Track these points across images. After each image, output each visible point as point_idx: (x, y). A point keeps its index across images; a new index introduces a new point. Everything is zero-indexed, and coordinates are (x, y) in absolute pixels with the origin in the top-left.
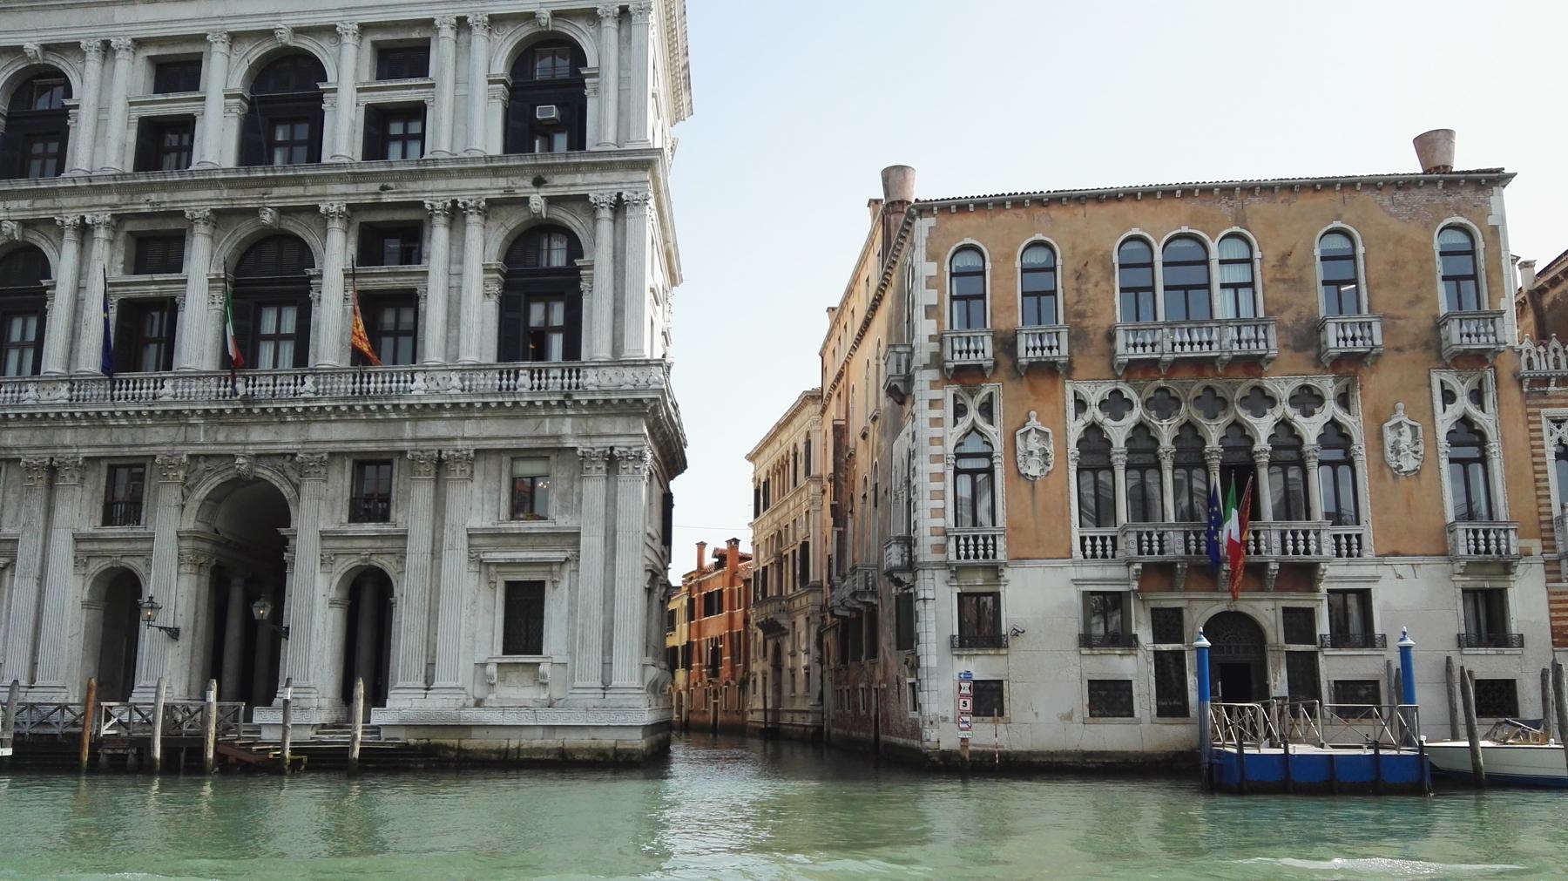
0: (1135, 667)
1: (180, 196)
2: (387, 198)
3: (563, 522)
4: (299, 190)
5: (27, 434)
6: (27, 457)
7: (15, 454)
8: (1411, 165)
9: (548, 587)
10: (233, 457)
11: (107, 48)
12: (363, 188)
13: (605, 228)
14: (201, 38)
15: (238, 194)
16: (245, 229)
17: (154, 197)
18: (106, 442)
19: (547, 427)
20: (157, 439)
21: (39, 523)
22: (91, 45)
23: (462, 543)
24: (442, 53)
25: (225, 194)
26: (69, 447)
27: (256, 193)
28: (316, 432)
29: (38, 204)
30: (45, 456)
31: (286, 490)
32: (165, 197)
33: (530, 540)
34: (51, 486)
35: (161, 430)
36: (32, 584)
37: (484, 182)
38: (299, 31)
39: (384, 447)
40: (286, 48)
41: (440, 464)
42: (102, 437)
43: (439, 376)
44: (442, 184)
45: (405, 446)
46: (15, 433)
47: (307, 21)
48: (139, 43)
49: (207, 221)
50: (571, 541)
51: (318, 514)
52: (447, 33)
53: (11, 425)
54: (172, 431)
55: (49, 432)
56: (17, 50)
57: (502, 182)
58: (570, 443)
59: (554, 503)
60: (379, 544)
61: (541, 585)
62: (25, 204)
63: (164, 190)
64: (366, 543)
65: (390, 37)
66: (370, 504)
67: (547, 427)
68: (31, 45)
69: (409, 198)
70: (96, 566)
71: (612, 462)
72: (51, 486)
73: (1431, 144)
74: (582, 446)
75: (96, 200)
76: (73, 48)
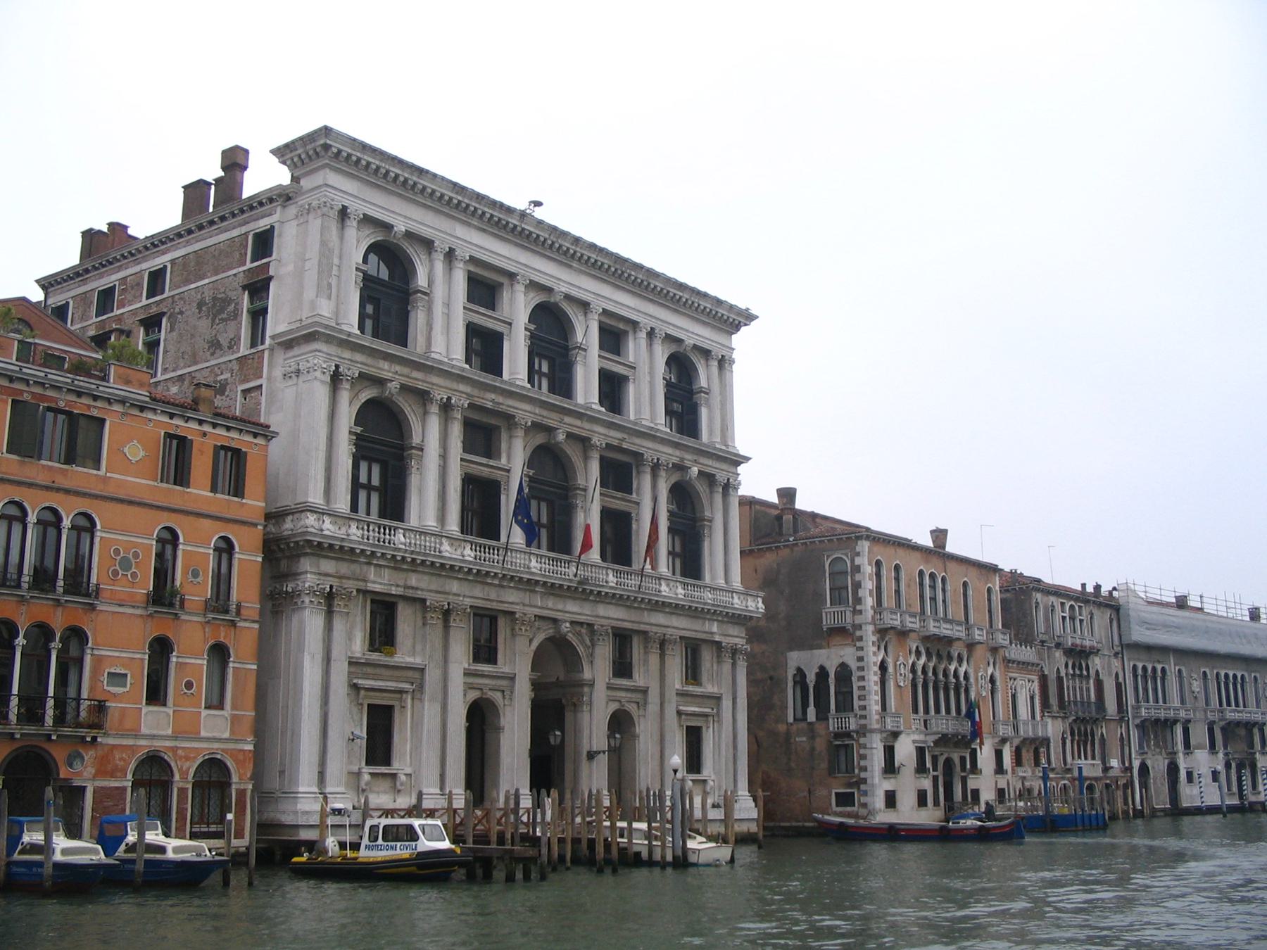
0: (926, 784)
1: (510, 402)
2: (625, 446)
3: (709, 688)
4: (578, 423)
5: (426, 578)
6: (431, 599)
7: (419, 594)
8: (928, 542)
9: (704, 729)
10: (555, 621)
11: (452, 251)
12: (613, 433)
13: (718, 498)
14: (512, 276)
15: (545, 413)
16: (540, 439)
17: (493, 396)
18: (481, 595)
19: (707, 627)
20: (511, 598)
21: (438, 656)
22: (441, 245)
23: (675, 698)
24: (635, 348)
25: (537, 411)
26: (459, 595)
27: (554, 415)
28: (602, 610)
29: (415, 374)
30: (443, 601)
31: (580, 649)
32: (501, 399)
34: (446, 626)
35: (515, 592)
36: (437, 707)
37: (669, 450)
38: (568, 297)
39: (635, 627)
40: (556, 304)
41: (663, 643)
42: (478, 591)
43: (672, 584)
44: (650, 444)
45: (647, 628)
46: (420, 576)
47: (574, 292)
48: (473, 260)
49: (527, 430)
50: (714, 701)
51: (597, 669)
52: (643, 335)
53: (420, 569)
54: (521, 594)
55: (442, 580)
56: (388, 227)
57: (678, 453)
58: (717, 638)
59: (704, 677)
60: (629, 695)
61: (390, 709)
62: (406, 370)
63: (502, 394)
64: (623, 694)
65: (613, 323)
66: (622, 668)
67: (707, 627)
68: (400, 227)
69: (634, 448)
70: (474, 695)
71: (734, 652)
72: (446, 626)
73: (940, 535)
74: (725, 641)
75: (455, 386)
76: (428, 244)
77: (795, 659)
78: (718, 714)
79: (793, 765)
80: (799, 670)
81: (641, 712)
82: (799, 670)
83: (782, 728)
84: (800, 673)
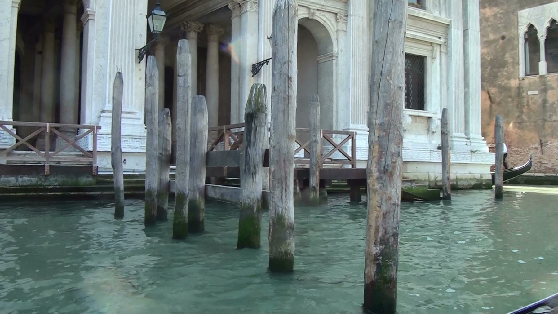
9: (429, 61)
33: (419, 24)
77: (526, 16)
78: (447, 44)
79: (525, 117)
80: (531, 27)
81: (341, 26)
82: (531, 27)
83: (514, 83)
84: (532, 30)
